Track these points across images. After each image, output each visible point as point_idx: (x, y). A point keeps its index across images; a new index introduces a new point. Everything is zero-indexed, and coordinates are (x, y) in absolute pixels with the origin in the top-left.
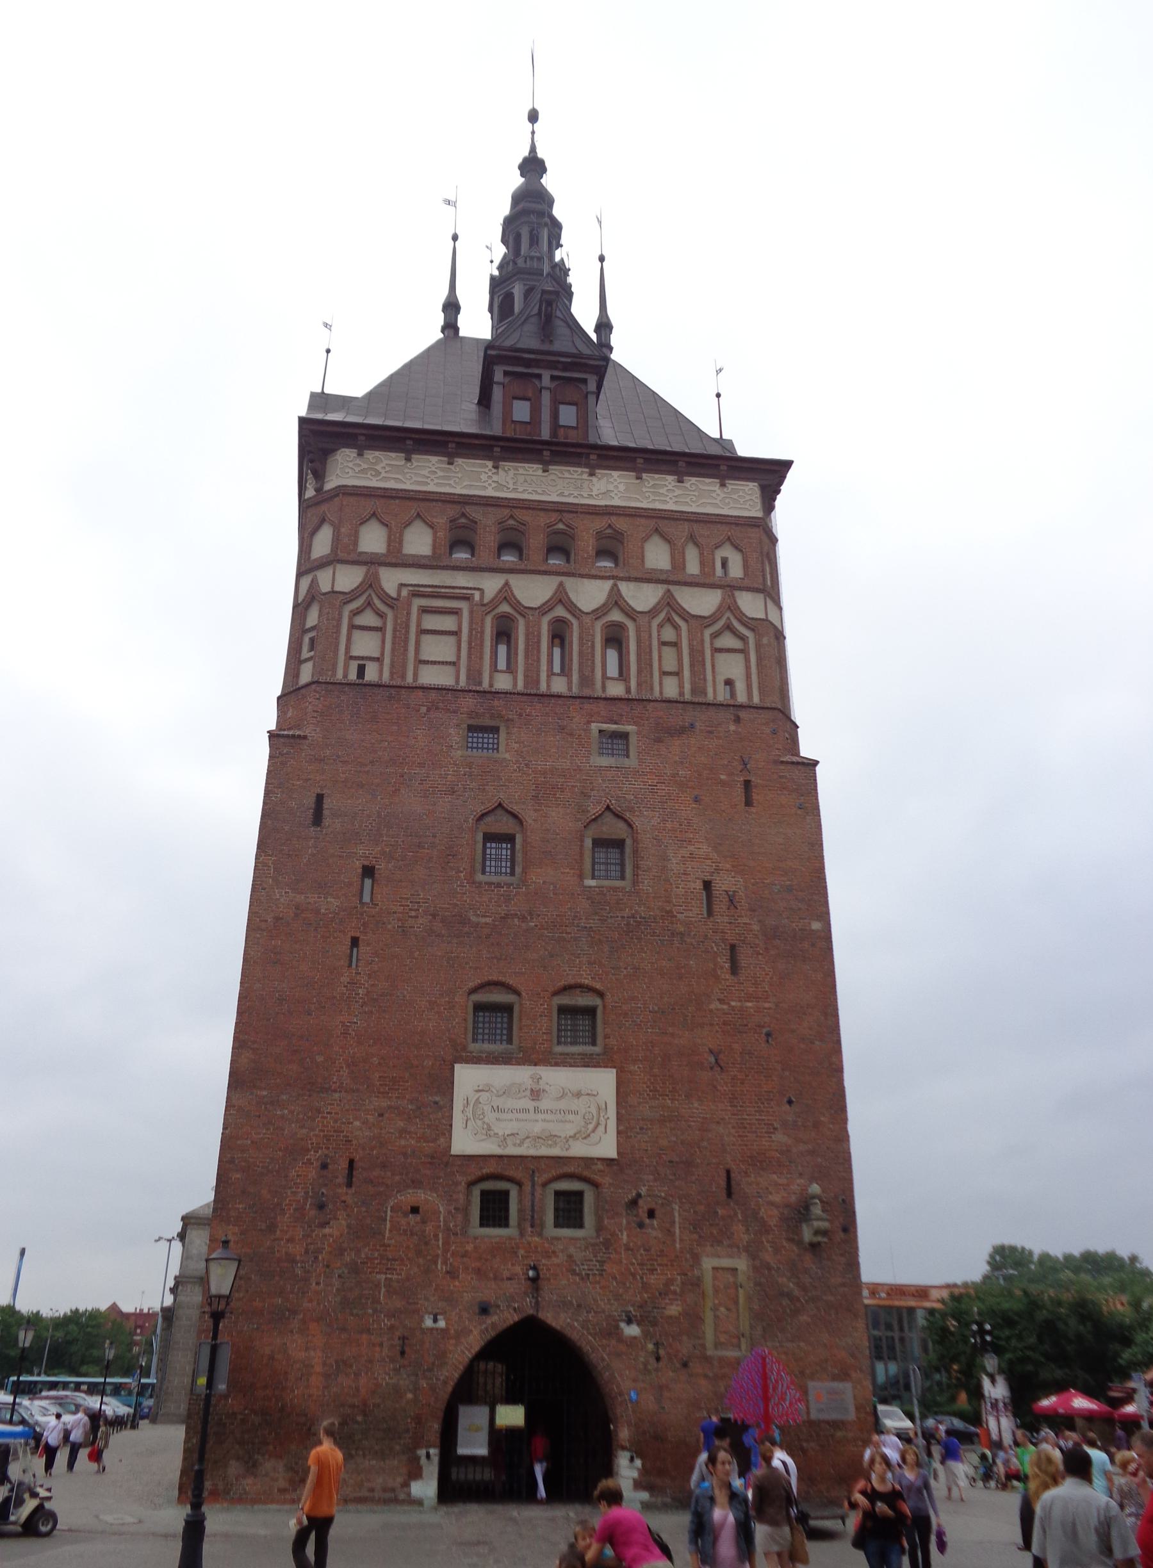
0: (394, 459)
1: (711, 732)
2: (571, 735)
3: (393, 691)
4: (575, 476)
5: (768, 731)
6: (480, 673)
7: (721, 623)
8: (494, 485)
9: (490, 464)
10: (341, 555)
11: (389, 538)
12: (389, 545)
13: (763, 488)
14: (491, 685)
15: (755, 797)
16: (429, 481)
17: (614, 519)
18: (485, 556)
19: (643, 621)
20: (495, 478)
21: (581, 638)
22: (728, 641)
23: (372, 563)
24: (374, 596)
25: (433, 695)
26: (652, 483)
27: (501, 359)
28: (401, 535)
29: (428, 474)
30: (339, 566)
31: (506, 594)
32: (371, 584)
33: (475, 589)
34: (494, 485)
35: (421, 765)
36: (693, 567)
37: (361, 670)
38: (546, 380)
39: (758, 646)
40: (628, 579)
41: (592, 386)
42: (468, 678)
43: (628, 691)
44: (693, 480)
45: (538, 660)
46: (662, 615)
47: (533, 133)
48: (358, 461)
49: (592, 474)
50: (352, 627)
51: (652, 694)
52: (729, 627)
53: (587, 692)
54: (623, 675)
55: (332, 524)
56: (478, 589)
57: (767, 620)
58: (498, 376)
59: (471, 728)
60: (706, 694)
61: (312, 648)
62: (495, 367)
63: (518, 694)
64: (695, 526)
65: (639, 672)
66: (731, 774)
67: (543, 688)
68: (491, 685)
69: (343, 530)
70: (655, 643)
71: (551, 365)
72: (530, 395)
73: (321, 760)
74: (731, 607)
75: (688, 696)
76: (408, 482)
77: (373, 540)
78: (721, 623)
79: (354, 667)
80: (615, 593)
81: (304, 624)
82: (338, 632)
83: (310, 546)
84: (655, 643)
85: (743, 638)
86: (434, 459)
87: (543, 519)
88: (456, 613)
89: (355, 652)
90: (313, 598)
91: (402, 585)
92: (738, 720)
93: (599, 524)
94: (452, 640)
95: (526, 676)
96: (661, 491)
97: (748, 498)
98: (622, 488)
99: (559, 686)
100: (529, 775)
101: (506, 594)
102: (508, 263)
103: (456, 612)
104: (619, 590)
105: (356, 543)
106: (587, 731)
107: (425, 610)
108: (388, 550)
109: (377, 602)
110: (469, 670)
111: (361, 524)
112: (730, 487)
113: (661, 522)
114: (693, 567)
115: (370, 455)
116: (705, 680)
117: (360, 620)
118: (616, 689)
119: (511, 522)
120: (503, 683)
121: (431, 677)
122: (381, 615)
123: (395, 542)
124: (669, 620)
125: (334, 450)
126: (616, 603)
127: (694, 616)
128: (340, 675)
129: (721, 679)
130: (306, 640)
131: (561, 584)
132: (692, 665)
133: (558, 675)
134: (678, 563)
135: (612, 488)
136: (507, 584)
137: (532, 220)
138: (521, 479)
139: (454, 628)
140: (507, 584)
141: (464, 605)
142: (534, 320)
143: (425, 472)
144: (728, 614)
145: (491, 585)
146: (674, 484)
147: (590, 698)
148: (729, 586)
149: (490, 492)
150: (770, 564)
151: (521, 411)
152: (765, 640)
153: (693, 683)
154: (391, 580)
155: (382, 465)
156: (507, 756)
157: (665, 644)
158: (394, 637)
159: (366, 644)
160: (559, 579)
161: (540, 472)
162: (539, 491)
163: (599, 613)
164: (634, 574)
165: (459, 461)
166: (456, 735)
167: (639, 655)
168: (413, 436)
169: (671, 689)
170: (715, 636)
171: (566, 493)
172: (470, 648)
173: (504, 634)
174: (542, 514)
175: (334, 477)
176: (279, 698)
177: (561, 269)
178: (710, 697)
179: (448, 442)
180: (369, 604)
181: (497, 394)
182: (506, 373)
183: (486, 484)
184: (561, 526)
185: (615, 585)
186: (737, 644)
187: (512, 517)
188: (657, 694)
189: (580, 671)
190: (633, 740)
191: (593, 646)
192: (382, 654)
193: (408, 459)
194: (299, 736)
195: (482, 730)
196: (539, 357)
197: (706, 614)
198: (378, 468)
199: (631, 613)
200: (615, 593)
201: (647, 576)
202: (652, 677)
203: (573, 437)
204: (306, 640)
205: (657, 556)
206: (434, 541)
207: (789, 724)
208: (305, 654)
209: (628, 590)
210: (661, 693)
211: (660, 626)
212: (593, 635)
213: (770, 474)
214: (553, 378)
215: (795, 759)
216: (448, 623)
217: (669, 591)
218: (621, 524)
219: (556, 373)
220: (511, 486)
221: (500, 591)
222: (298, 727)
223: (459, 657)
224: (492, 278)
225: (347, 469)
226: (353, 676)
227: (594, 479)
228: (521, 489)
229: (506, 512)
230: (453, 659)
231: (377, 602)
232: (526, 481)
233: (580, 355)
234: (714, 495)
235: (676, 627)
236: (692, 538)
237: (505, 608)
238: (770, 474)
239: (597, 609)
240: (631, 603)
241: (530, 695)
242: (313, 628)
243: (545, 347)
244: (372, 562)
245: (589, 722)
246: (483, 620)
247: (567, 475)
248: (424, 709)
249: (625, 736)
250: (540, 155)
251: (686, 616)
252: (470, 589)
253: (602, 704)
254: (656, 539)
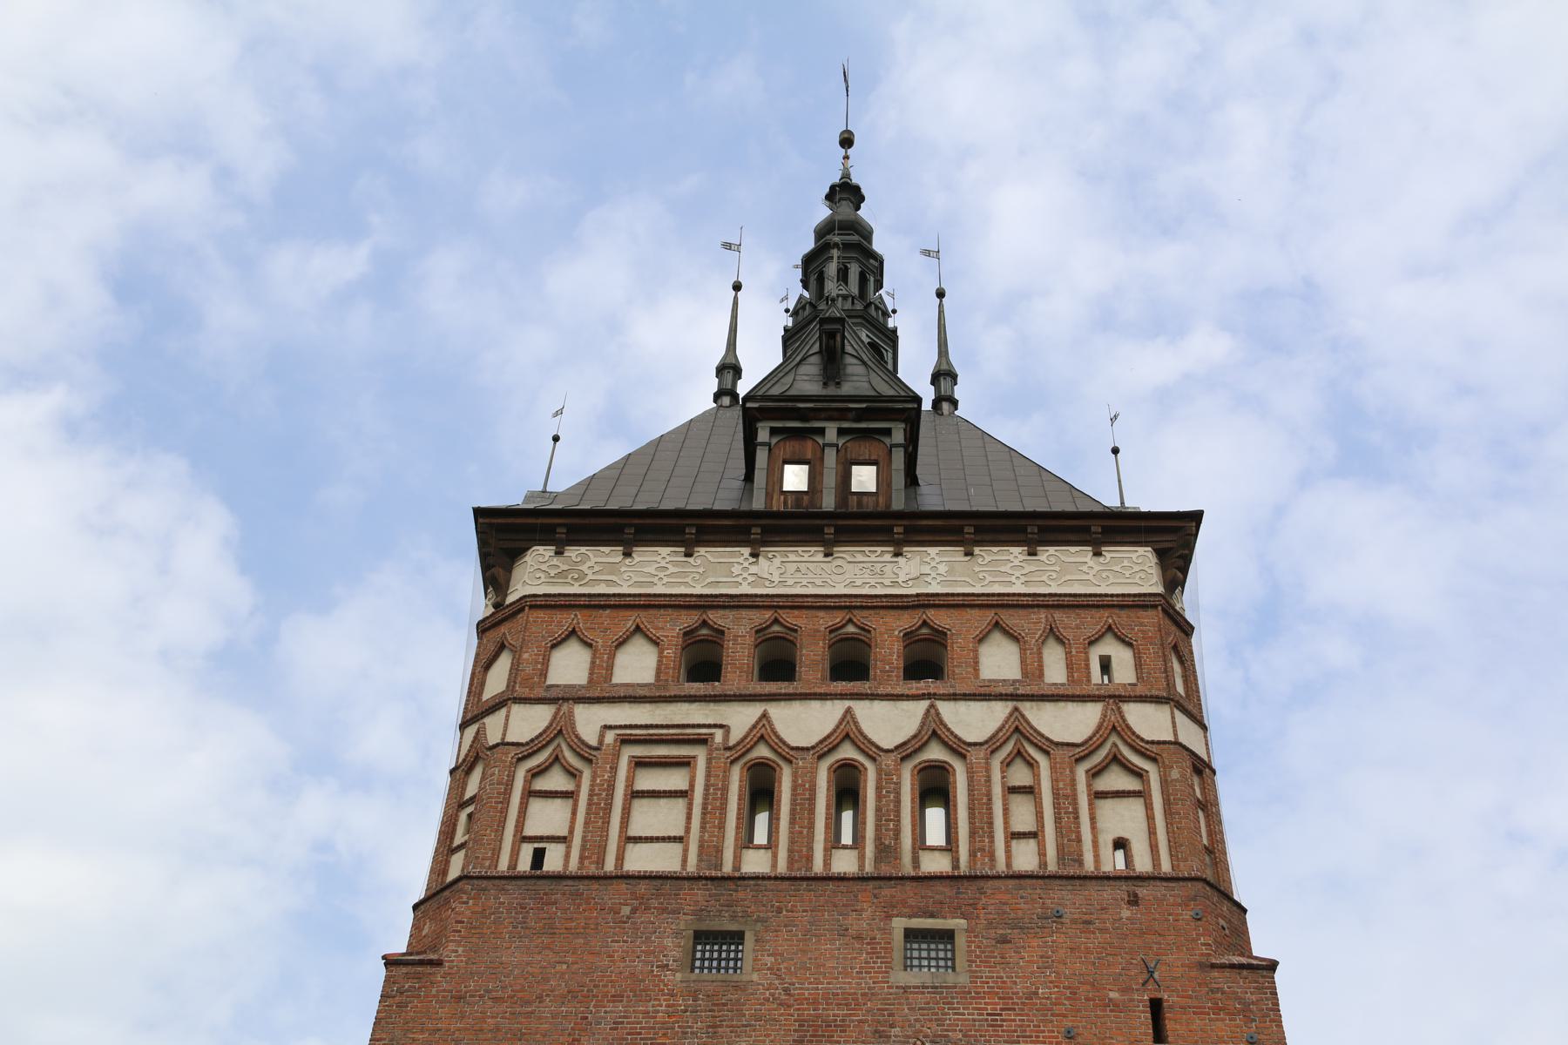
0: (609, 555)
1: (1089, 922)
2: (859, 938)
3: (581, 886)
4: (873, 558)
5: (1187, 915)
6: (719, 851)
7: (1103, 753)
8: (751, 579)
9: (746, 551)
10: (520, 691)
11: (593, 663)
12: (591, 674)
13: (1161, 554)
14: (737, 867)
15: (1169, 1025)
16: (655, 580)
17: (931, 613)
18: (733, 680)
19: (976, 756)
20: (753, 569)
21: (879, 788)
22: (1116, 780)
23: (565, 700)
24: (564, 747)
25: (643, 887)
26: (988, 559)
27: (766, 414)
28: (612, 657)
29: (657, 570)
30: (517, 710)
31: (763, 732)
32: (560, 731)
33: (715, 726)
34: (751, 579)
35: (617, 998)
36: (1055, 670)
37: (539, 856)
38: (831, 434)
39: (1164, 783)
40: (954, 697)
41: (898, 436)
42: (700, 860)
43: (956, 865)
44: (1052, 550)
45: (811, 826)
46: (1009, 747)
47: (846, 157)
48: (555, 561)
49: (897, 554)
50: (530, 794)
51: (992, 867)
52: (1116, 759)
53: (886, 870)
54: (951, 846)
55: (513, 652)
56: (721, 726)
57: (1177, 743)
58: (763, 435)
59: (701, 937)
60: (1080, 862)
61: (468, 831)
62: (759, 425)
63: (776, 878)
64: (1058, 614)
65: (973, 834)
66: (1125, 990)
67: (818, 867)
68: (737, 867)
69: (526, 656)
70: (997, 790)
71: (840, 415)
72: (809, 456)
73: (459, 998)
74: (1116, 728)
75: (1052, 867)
76: (625, 585)
77: (570, 666)
78: (1103, 753)
79: (527, 851)
80: (932, 715)
81: (463, 794)
82: (507, 801)
83: (483, 684)
84: (997, 790)
85: (1139, 774)
86: (664, 551)
87: (825, 620)
88: (687, 764)
89: (529, 831)
90: (477, 758)
91: (607, 727)
92: (1134, 901)
93: (908, 621)
94: (680, 804)
95: (790, 851)
96: (1003, 569)
97: (1137, 568)
98: (942, 569)
99: (845, 863)
100: (789, 1006)
101: (763, 732)
102: (803, 308)
103: (685, 763)
104: (938, 714)
105: (544, 674)
106: (887, 931)
107: (640, 764)
108: (590, 680)
109: (569, 755)
110: (701, 847)
111: (554, 646)
112: (1108, 555)
113: (1000, 610)
114: (1055, 670)
115: (573, 552)
116: (1079, 840)
117: (541, 784)
118: (936, 864)
119: (776, 628)
120: (756, 863)
121: (641, 860)
122: (573, 774)
123: (602, 669)
124: (1019, 753)
125: (522, 551)
126: (934, 732)
127: (1057, 744)
128: (503, 865)
129: (1106, 841)
130: (463, 816)
131: (848, 711)
132: (1058, 820)
133: (845, 847)
134: (1032, 668)
135: (930, 570)
136: (765, 715)
137: (842, 254)
138: (792, 568)
139: (684, 786)
140: (765, 715)
141: (700, 753)
142: (815, 359)
143: (651, 569)
144: (1114, 738)
145: (740, 718)
146: (1022, 557)
147: (890, 878)
148: (1110, 697)
149: (745, 589)
150: (1182, 662)
151: (795, 478)
152: (1175, 774)
153: (1060, 849)
154: (589, 721)
155: (589, 564)
156: (755, 977)
157: (1013, 790)
158: (590, 804)
159: (547, 818)
160: (847, 703)
161: (820, 557)
162: (818, 582)
163: (906, 751)
164: (961, 689)
165: (702, 550)
166: (673, 946)
167: (971, 810)
168: (637, 521)
169: (1025, 858)
170: (1095, 773)
171: (859, 583)
172: (704, 814)
173: (761, 793)
174: (821, 614)
175: (519, 586)
176: (415, 907)
177: (877, 308)
178: (1089, 865)
179: (684, 527)
180: (556, 759)
181: (762, 456)
182: (773, 431)
183: (739, 579)
184: (851, 629)
185: (932, 706)
186: (1130, 784)
187: (776, 621)
188: (1001, 866)
189: (878, 839)
190: (961, 940)
191: (898, 802)
192: (571, 831)
193: (627, 554)
194: (431, 963)
195: (716, 940)
196: (819, 405)
197: (1078, 739)
198: (584, 568)
199: (959, 748)
200: (932, 715)
201: (982, 690)
202: (992, 842)
203: (869, 506)
204: (463, 816)
205: (999, 661)
206: (660, 662)
207: (1225, 907)
208: (459, 839)
209: (950, 712)
210: (1009, 865)
211: (1007, 764)
212: (898, 784)
213: (1172, 536)
214: (841, 432)
215: (1243, 960)
216: (674, 780)
217: (1016, 709)
218: (940, 619)
219: (846, 425)
220: (776, 579)
221: (754, 727)
222: (434, 949)
223: (688, 830)
224: (786, 330)
225: (538, 572)
226: (524, 864)
227: (900, 559)
228: (790, 582)
229: (768, 615)
230: (680, 833)
231: (569, 755)
232: (798, 570)
233: (879, 398)
234: (1085, 568)
235: (1031, 764)
236: (1053, 633)
237: (762, 751)
238: (1172, 536)
239: (904, 744)
240: (957, 732)
241: (795, 879)
242: (472, 800)
243: (831, 391)
245: (889, 917)
246: (727, 772)
247: (860, 557)
248: (626, 910)
249: (948, 936)
250: (855, 180)
251: (1047, 746)
252: (709, 726)
253: (909, 885)
254: (997, 637)
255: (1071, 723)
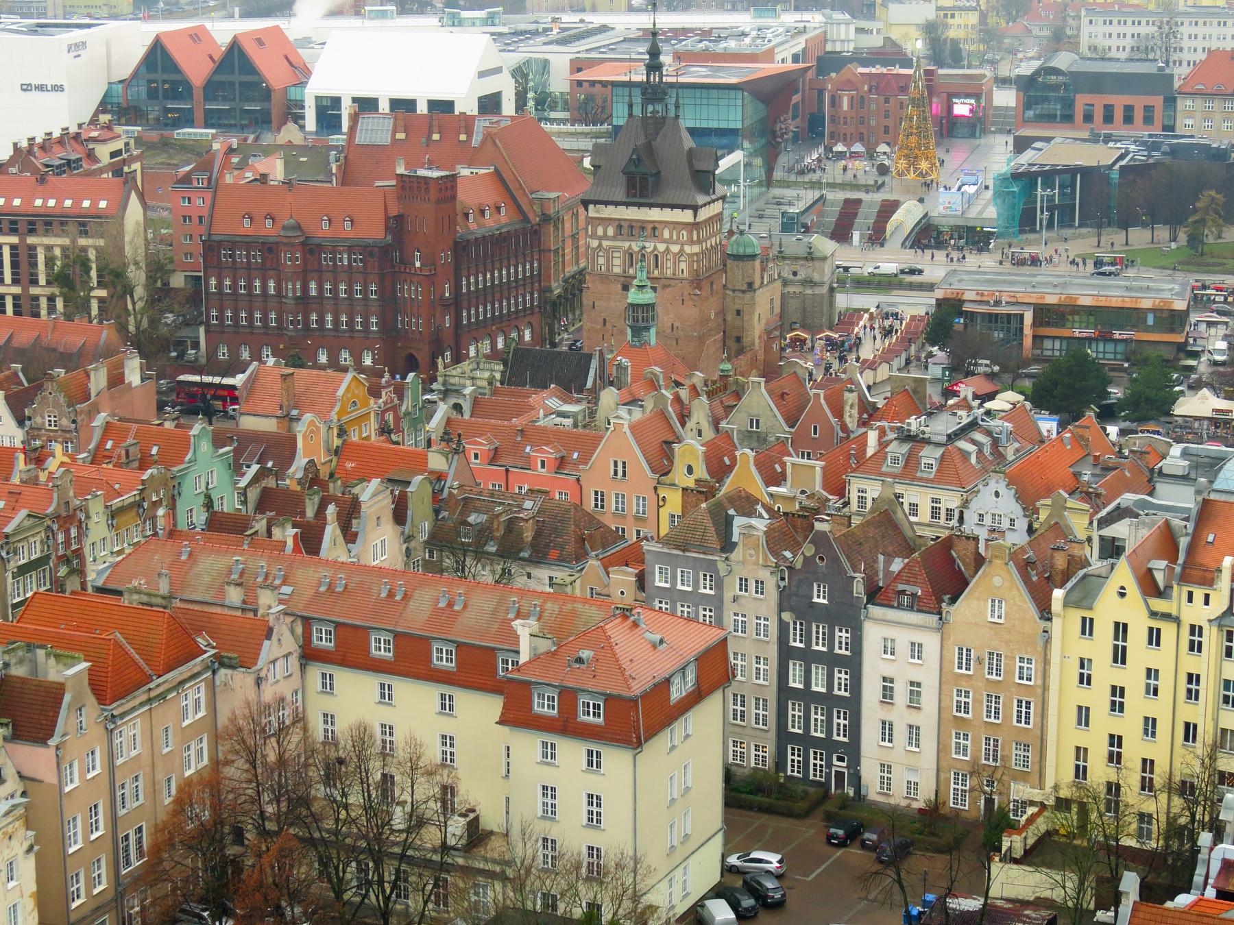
31: (630, 247)
32: (600, 245)
74: (682, 250)
101: (630, 247)
113: (666, 223)
123: (605, 232)
134: (671, 237)
145: (627, 245)
154: (605, 243)
225: (593, 211)
244: (600, 238)
255: (675, 248)
